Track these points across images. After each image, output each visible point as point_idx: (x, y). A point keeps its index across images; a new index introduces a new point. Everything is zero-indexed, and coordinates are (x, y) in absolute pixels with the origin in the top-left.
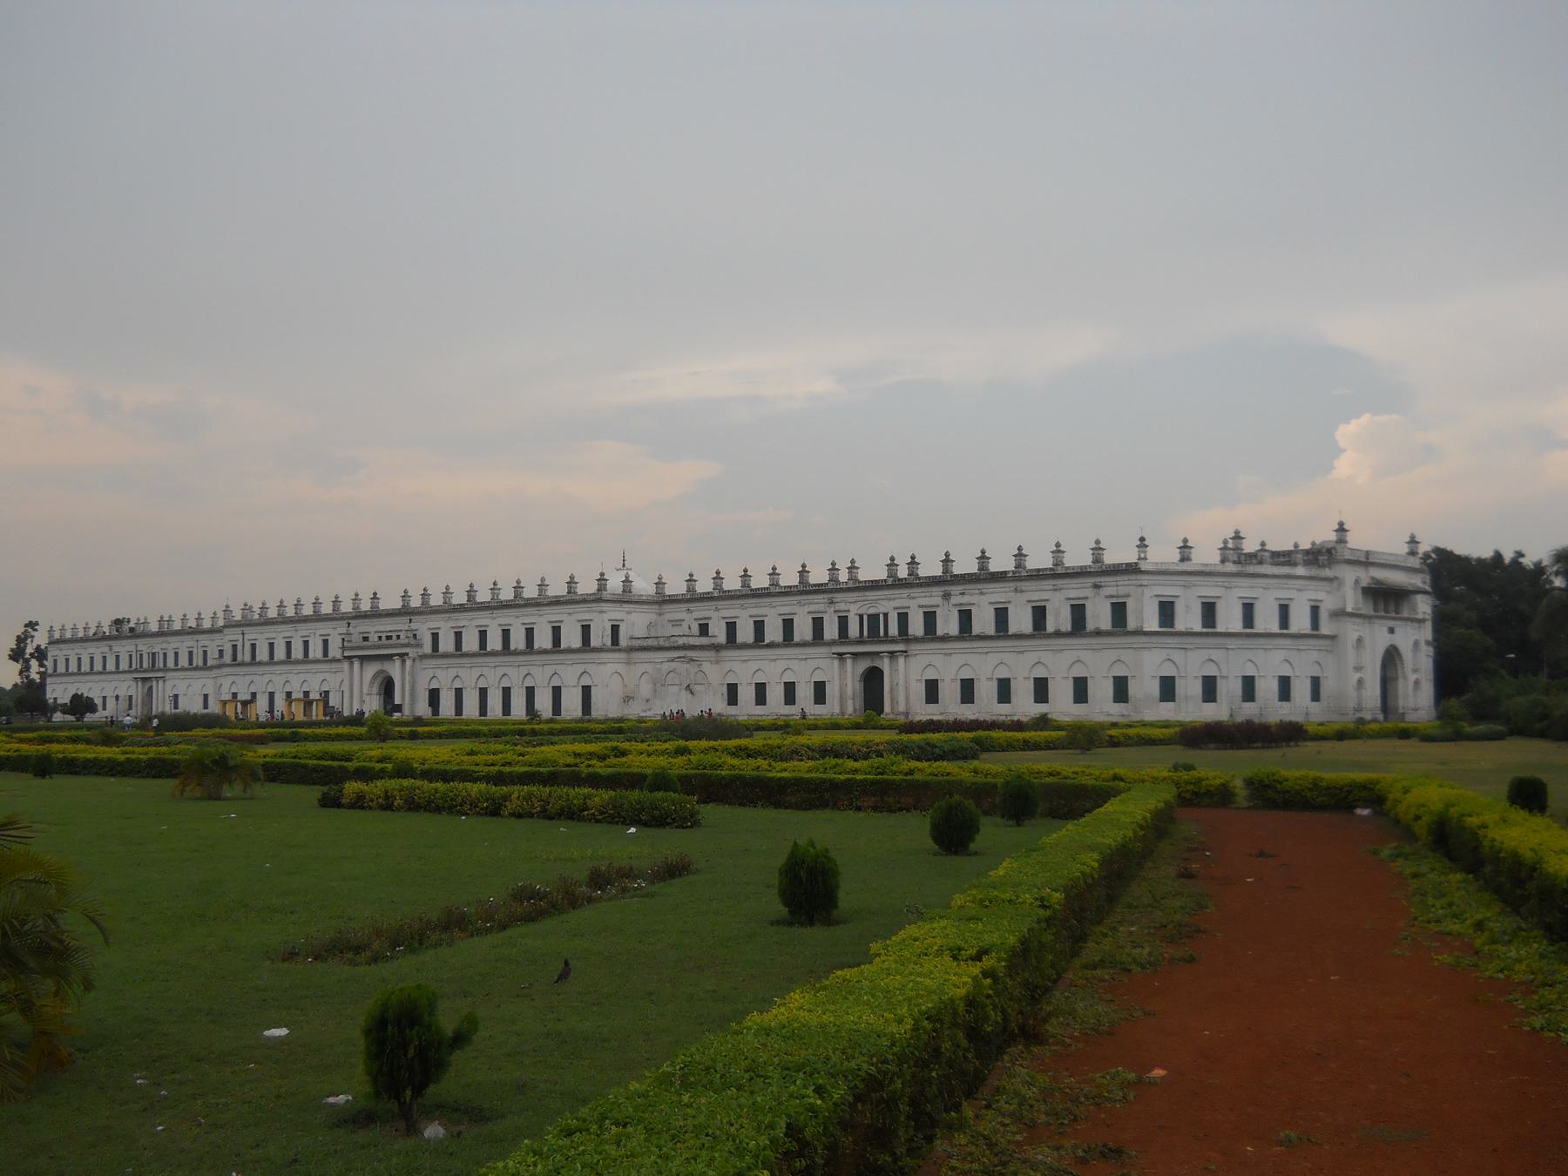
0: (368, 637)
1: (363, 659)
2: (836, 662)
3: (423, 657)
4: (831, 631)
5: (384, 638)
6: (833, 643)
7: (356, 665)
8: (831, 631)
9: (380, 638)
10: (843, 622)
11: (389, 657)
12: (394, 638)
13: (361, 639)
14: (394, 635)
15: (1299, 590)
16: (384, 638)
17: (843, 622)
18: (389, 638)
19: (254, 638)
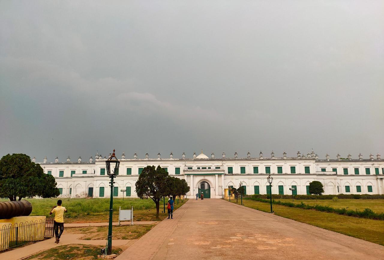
0: (210, 168)
1: (194, 175)
2: (379, 180)
3: (225, 175)
4: (373, 172)
5: (201, 168)
6: (374, 175)
7: (192, 177)
8: (373, 172)
9: (199, 168)
10: (377, 170)
11: (214, 175)
12: (207, 168)
13: (197, 169)
14: (207, 168)
15: (361, 165)
16: (201, 168)
17: (377, 170)
18: (209, 168)
19: (210, 165)
